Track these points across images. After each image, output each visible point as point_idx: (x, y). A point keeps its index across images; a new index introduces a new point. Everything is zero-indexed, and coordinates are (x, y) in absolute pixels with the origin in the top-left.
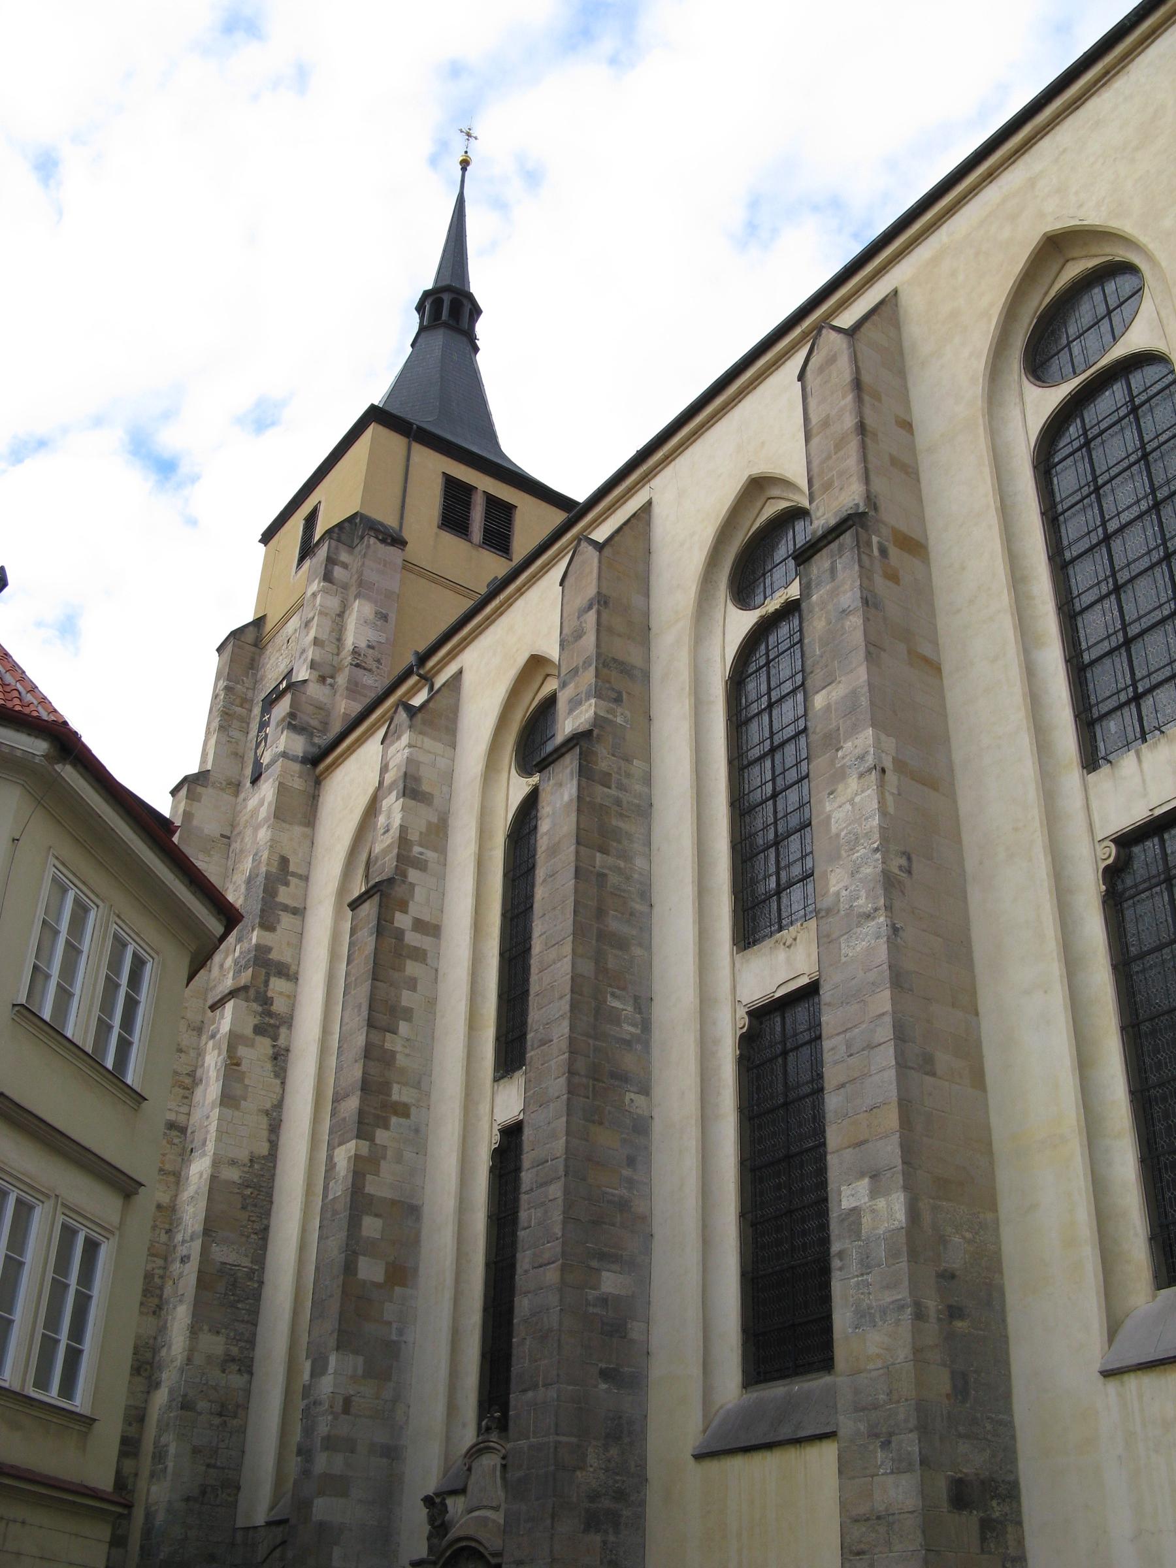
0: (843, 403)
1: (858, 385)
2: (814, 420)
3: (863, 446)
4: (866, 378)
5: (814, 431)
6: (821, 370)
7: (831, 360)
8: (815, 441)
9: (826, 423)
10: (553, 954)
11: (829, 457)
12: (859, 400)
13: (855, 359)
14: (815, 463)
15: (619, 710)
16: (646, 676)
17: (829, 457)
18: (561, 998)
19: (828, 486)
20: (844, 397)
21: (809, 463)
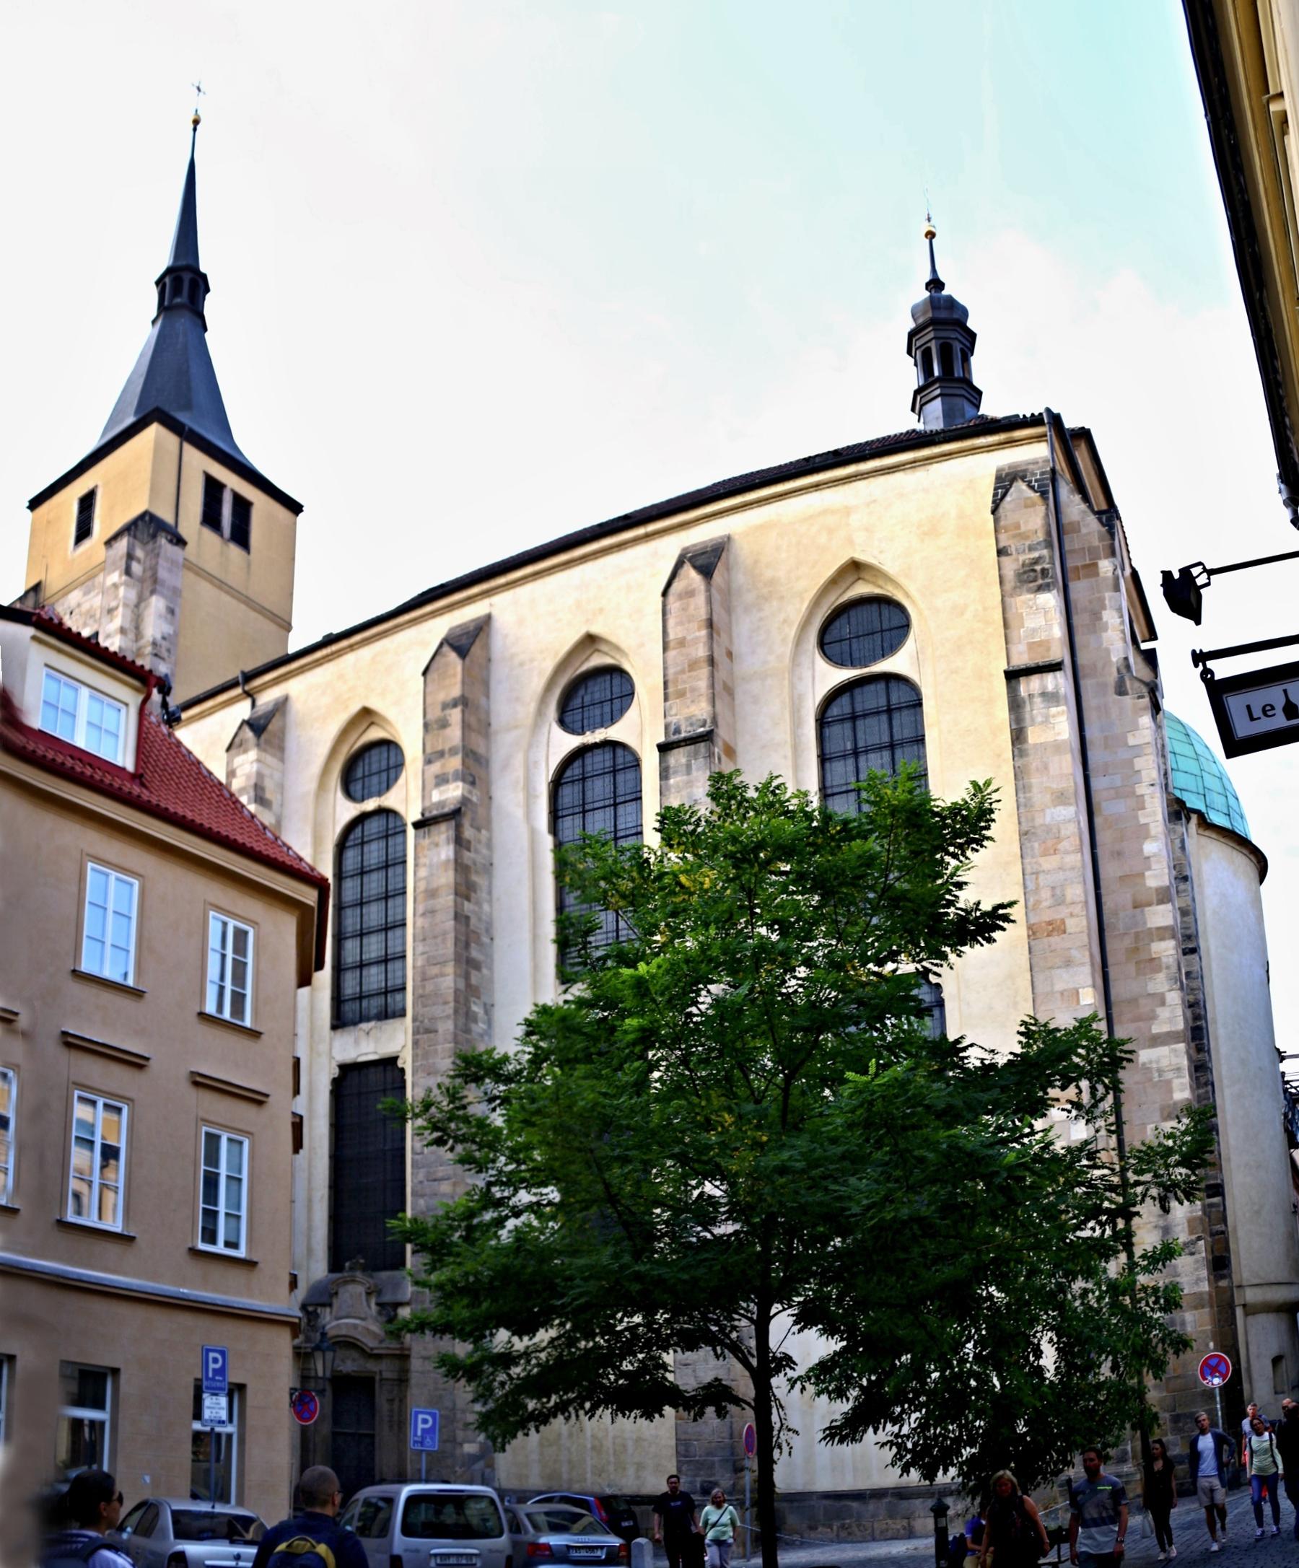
0: (697, 634)
1: (710, 624)
2: (672, 636)
3: (712, 676)
4: (715, 618)
5: (672, 645)
6: (681, 597)
7: (690, 593)
8: (672, 654)
9: (682, 643)
10: (435, 970)
11: (683, 672)
12: (711, 637)
13: (709, 601)
14: (671, 671)
15: (475, 791)
16: (487, 761)
17: (683, 672)
18: (446, 1003)
19: (681, 694)
20: (699, 629)
21: (665, 669)
